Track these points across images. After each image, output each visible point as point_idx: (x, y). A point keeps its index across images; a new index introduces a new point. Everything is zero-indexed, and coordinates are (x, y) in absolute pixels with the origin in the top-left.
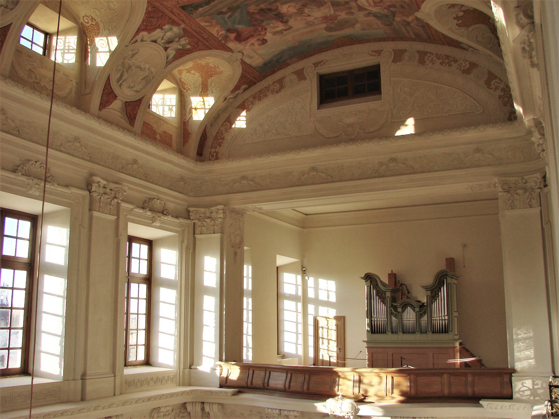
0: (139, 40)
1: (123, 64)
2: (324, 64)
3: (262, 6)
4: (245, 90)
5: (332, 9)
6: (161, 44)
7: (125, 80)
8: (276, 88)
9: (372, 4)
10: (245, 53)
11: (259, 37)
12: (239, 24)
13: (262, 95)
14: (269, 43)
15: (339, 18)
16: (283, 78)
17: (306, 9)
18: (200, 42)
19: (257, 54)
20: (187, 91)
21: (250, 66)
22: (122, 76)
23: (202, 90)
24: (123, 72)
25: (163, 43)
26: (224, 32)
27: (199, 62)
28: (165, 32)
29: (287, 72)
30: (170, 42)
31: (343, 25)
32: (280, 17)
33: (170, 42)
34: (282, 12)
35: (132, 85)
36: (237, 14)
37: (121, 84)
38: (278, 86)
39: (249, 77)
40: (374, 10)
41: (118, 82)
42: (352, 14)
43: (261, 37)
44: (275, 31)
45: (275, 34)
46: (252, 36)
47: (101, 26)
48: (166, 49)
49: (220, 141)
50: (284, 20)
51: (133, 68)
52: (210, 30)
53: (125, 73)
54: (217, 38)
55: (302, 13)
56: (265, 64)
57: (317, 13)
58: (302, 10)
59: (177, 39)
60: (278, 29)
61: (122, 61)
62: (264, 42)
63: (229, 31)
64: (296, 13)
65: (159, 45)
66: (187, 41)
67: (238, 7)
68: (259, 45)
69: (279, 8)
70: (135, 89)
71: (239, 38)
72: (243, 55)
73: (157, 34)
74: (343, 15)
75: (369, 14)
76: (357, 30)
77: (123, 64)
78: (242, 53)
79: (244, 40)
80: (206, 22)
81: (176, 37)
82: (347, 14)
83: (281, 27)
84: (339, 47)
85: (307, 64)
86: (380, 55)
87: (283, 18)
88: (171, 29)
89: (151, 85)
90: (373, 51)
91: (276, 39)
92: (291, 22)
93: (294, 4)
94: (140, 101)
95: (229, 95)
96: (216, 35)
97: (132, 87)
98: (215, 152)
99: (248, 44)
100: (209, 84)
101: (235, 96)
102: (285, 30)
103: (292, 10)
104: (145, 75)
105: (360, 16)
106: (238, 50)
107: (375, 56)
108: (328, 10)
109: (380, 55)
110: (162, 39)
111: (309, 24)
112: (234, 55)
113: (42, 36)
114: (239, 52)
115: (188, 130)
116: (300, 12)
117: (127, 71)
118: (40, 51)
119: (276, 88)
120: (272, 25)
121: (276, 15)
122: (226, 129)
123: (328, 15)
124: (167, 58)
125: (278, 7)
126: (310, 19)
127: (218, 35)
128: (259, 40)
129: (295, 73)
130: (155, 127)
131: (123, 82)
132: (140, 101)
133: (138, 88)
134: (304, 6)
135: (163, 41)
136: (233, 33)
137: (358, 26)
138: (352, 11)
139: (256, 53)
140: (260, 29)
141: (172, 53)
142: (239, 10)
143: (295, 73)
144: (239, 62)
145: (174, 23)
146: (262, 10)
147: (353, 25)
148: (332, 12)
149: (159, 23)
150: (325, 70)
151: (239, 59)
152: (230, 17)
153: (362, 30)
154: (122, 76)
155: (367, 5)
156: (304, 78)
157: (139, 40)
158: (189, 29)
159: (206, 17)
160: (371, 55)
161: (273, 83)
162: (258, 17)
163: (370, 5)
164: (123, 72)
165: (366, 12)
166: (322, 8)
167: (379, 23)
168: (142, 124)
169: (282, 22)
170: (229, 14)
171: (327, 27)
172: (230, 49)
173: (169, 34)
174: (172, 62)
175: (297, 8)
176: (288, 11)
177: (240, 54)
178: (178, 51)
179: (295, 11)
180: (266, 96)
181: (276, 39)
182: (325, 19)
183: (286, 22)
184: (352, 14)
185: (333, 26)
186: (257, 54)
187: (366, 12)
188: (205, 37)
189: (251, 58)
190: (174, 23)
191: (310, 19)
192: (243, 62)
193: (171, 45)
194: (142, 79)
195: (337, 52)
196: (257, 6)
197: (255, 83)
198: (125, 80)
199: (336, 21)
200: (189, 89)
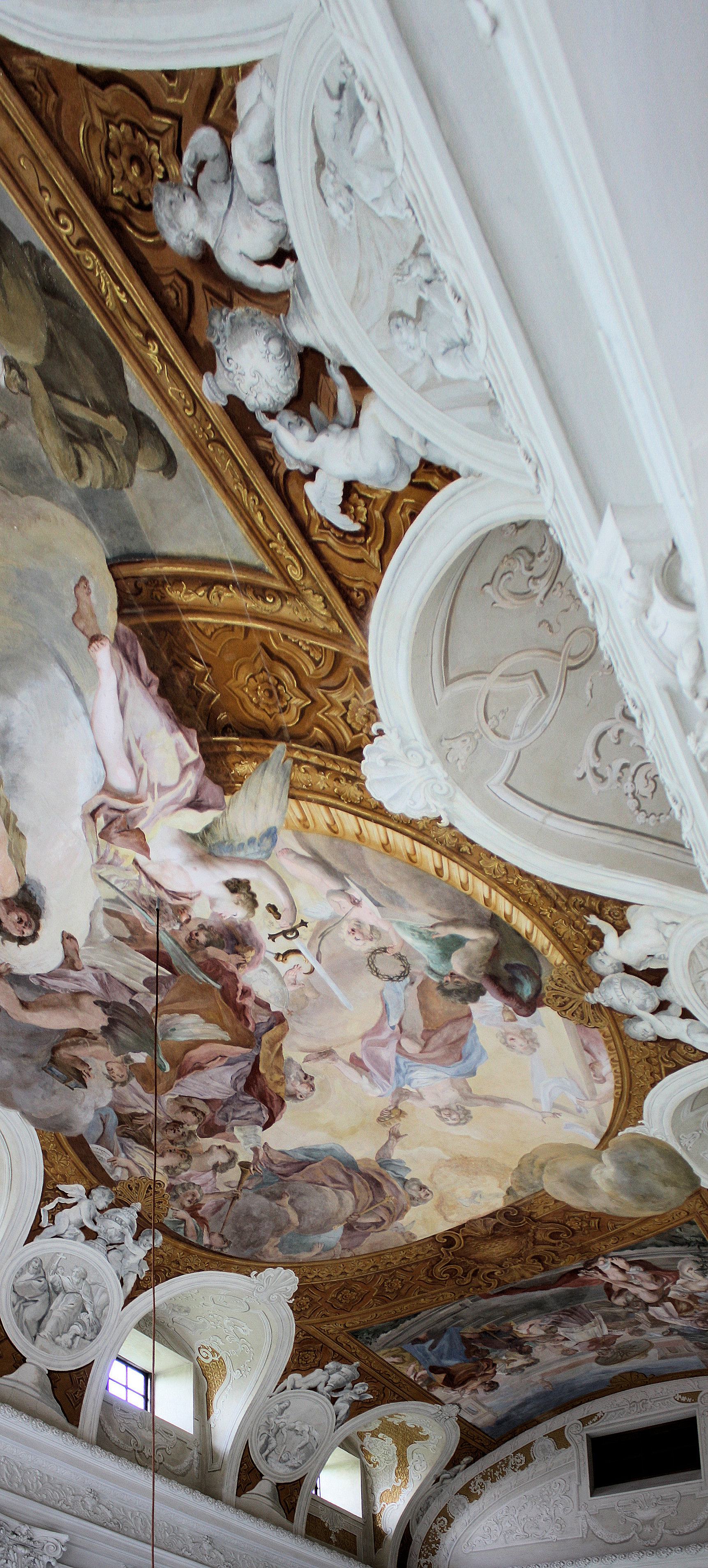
0: (289, 1387)
1: (268, 1424)
2: (599, 1419)
3: (485, 1327)
4: (468, 1465)
5: (604, 1325)
6: (325, 1392)
7: (273, 1450)
8: (519, 1461)
9: (676, 1314)
10: (463, 1405)
11: (484, 1379)
12: (449, 1358)
13: (497, 1474)
14: (502, 1387)
15: (618, 1341)
16: (531, 1444)
17: (559, 1329)
18: (385, 1387)
19: (483, 1406)
20: (374, 1466)
21: (473, 1427)
22: (267, 1443)
23: (399, 1464)
24: (269, 1437)
25: (328, 1392)
26: (424, 1372)
27: (390, 1420)
28: (329, 1374)
29: (536, 1434)
30: (339, 1389)
31: (625, 1353)
32: (518, 1345)
33: (339, 1389)
34: (520, 1336)
35: (284, 1458)
36: (444, 1342)
37: (267, 1457)
38: (523, 1458)
39: (473, 1444)
40: (679, 1323)
41: (261, 1453)
42: (641, 1332)
43: (488, 1380)
44: (510, 1366)
45: (510, 1372)
46: (472, 1377)
47: (228, 1364)
48: (333, 1401)
49: (434, 1546)
50: (525, 1349)
51: (284, 1430)
52: (402, 1368)
53: (272, 1438)
54: (414, 1382)
55: (553, 1336)
56: (499, 1423)
57: (577, 1335)
58: (553, 1330)
59: (350, 1385)
60: (516, 1364)
61: (266, 1419)
62: (493, 1386)
63: (434, 1369)
64: (542, 1336)
65: (322, 1394)
66: (367, 1388)
67: (445, 1330)
68: (485, 1391)
69: (514, 1329)
70: (289, 1463)
71: (452, 1381)
72: (460, 1408)
73: (317, 1376)
74: (624, 1336)
75: (671, 1332)
76: (651, 1360)
77: (268, 1424)
78: (459, 1405)
79: (460, 1386)
80: (394, 1356)
81: (348, 1382)
82: (631, 1334)
83: (520, 1360)
84: (622, 1389)
85: (569, 1419)
86: (696, 1401)
87: (522, 1346)
88: (338, 1370)
89: (314, 1456)
90: (682, 1395)
91: (514, 1382)
92: (537, 1352)
93: (538, 1321)
94: (300, 1481)
95: (443, 1473)
96: (412, 1377)
97: (285, 1462)
98: (427, 1563)
99: (467, 1391)
100: (409, 1456)
101: (453, 1474)
102: (528, 1365)
103: (537, 1331)
104: (303, 1443)
105: (656, 1335)
106: (451, 1401)
107: (686, 1402)
108: (598, 1329)
109: (696, 1401)
110: (326, 1385)
111: (567, 1352)
112: (444, 1408)
113: (141, 1377)
114: (453, 1404)
115: (380, 1529)
116: (550, 1334)
117: (275, 1437)
118: (139, 1403)
119: (519, 1461)
120: (504, 1358)
121: (509, 1341)
122: (442, 1528)
123: (599, 1336)
124: (337, 1416)
125: (511, 1328)
126: (567, 1345)
127: (415, 1376)
128: (484, 1383)
129: (549, 1435)
130: (327, 1522)
131: (270, 1453)
132: (300, 1481)
133: (295, 1462)
134: (557, 1323)
135: (327, 1388)
136: (440, 1373)
137: (653, 1352)
138: (640, 1327)
139: (481, 1406)
140: (485, 1365)
141: (343, 1407)
142: (446, 1336)
143: (549, 1435)
144: (454, 1420)
145: (342, 1359)
146: (485, 1332)
147: (644, 1353)
148: (606, 1332)
149: (318, 1359)
150: (599, 1429)
151: (454, 1415)
152: (432, 1347)
153: (662, 1358)
154: (267, 1443)
155: (667, 1315)
156: (567, 1445)
157: (289, 1387)
158: (368, 1369)
159: (393, 1349)
160: (680, 1401)
161: (515, 1454)
162: (480, 1346)
163: (671, 1316)
164: (269, 1437)
165: (665, 1328)
166: (587, 1326)
167: (691, 1345)
168: (305, 1518)
169: (521, 1352)
170: (431, 1342)
171: (598, 1358)
172: (437, 1399)
173: (336, 1377)
174: (345, 1421)
175: (544, 1327)
176: (530, 1334)
177: (455, 1407)
178: (353, 1403)
179: (543, 1333)
180: (503, 1474)
181: (514, 1382)
182: (595, 1343)
183: (527, 1352)
184: (641, 1332)
185: (609, 1355)
186: (483, 1406)
187: (665, 1328)
188: (395, 1381)
189: (474, 1413)
190: (342, 1359)
191: (567, 1345)
192: (461, 1421)
193: (340, 1394)
194: (300, 1449)
195: (620, 1398)
196: (478, 1327)
197: (484, 1454)
198: (273, 1450)
199: (613, 1347)
200: (377, 1463)
